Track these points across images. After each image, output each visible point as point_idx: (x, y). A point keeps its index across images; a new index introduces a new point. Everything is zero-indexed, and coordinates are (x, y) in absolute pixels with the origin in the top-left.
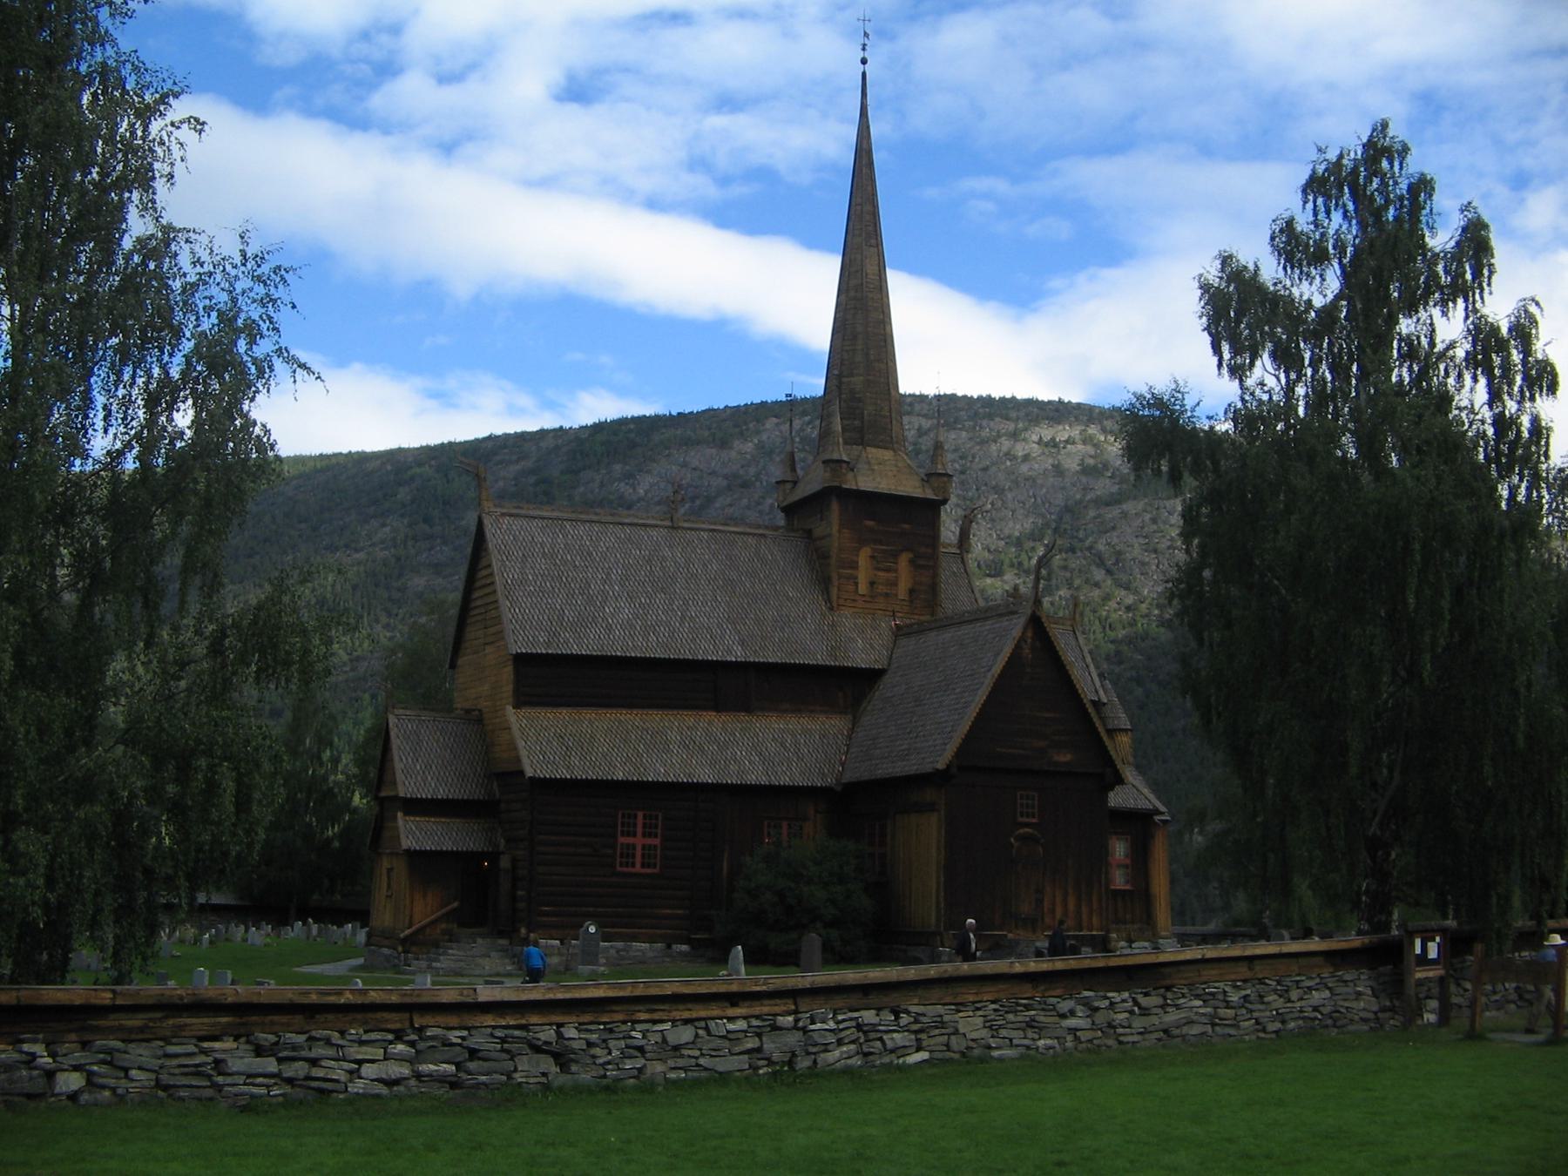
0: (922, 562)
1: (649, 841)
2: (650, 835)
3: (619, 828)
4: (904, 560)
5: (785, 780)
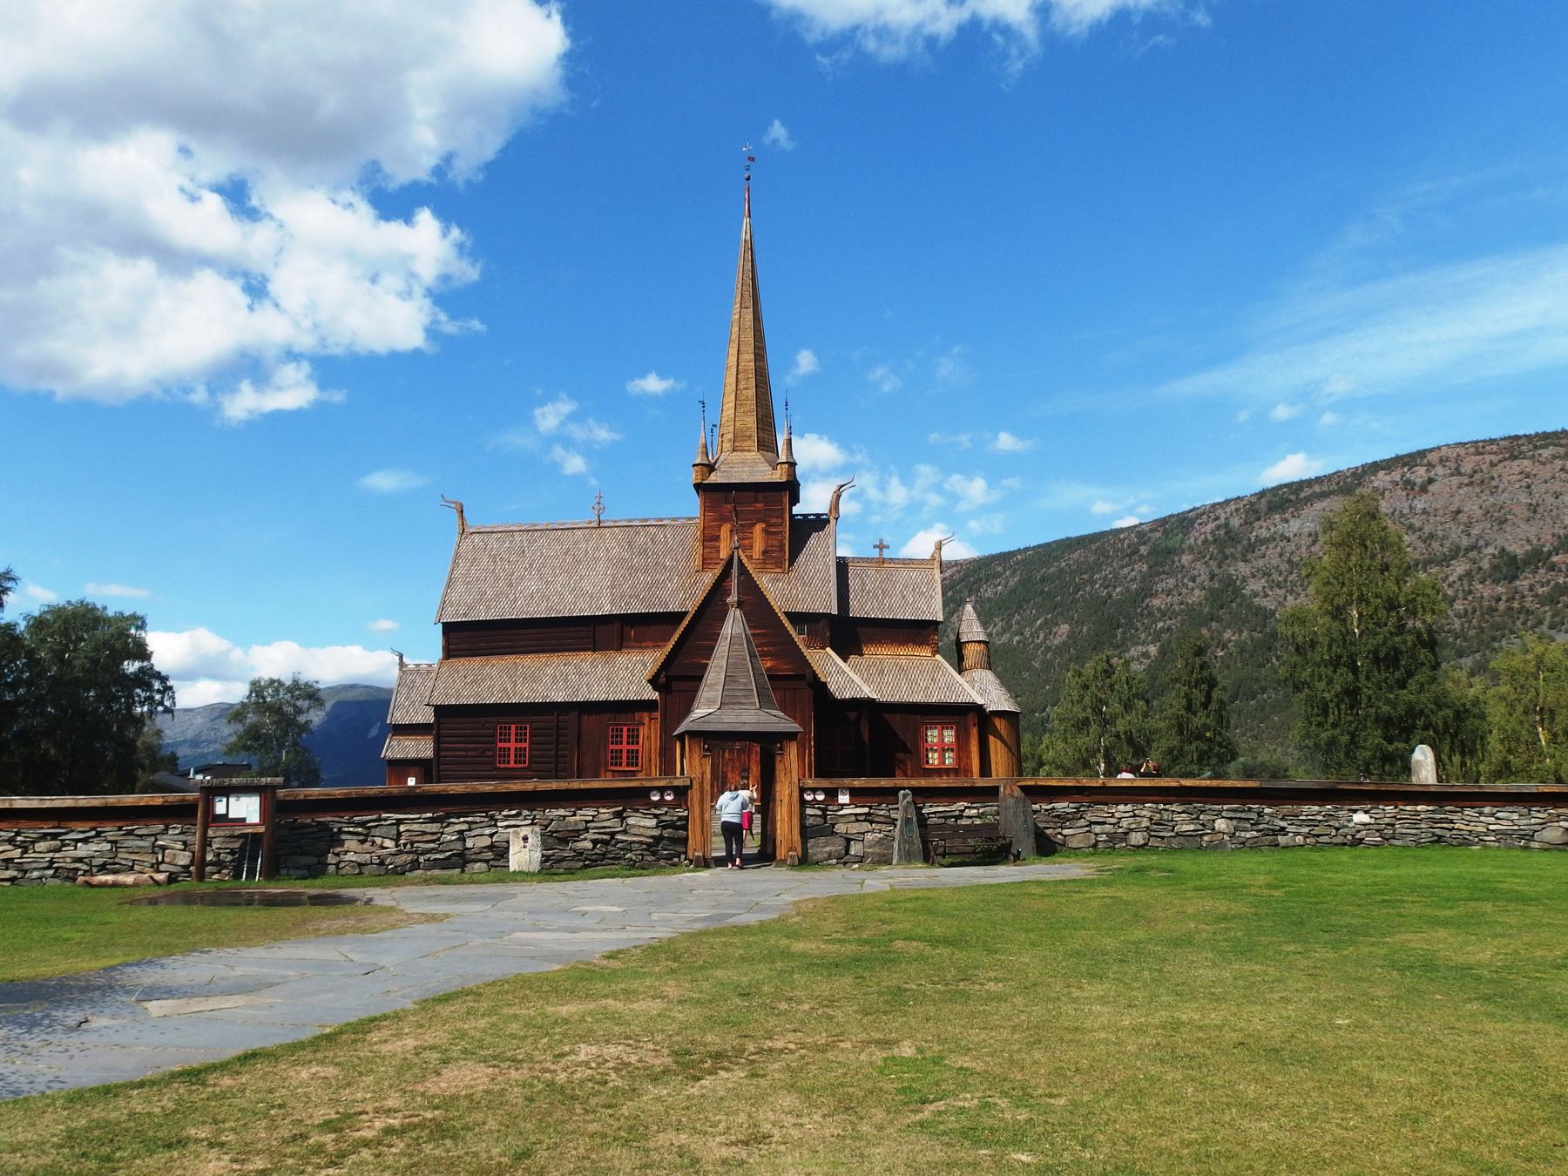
1: (519, 745)
2: (521, 742)
4: (758, 529)
5: (622, 697)
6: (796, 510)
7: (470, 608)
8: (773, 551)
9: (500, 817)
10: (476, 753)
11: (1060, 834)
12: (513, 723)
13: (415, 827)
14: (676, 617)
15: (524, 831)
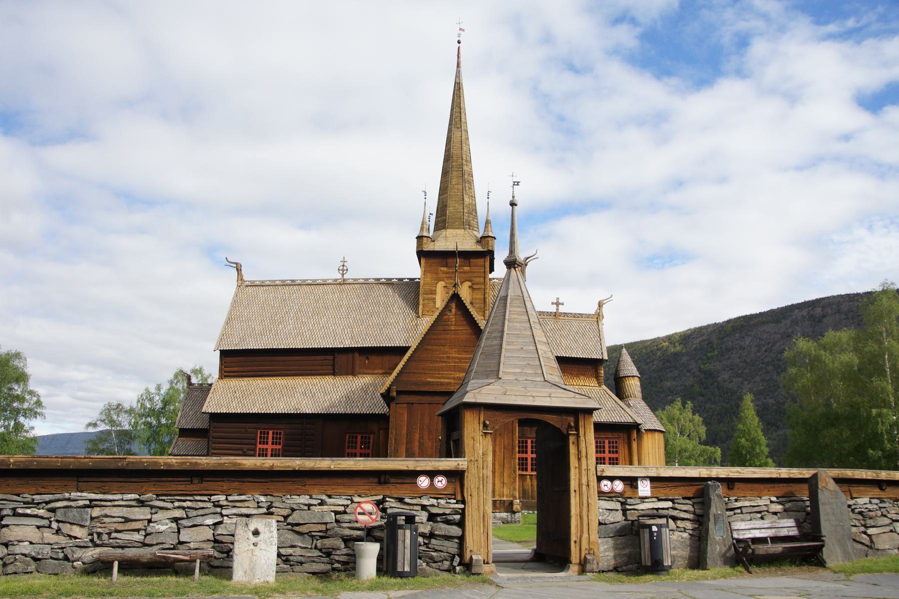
0: (475, 286)
1: (275, 447)
3: (258, 440)
5: (357, 411)
6: (491, 276)
7: (243, 339)
8: (476, 303)
9: (225, 503)
10: (241, 452)
11: (865, 533)
12: (271, 429)
13: (116, 512)
14: (400, 351)
15: (254, 524)
